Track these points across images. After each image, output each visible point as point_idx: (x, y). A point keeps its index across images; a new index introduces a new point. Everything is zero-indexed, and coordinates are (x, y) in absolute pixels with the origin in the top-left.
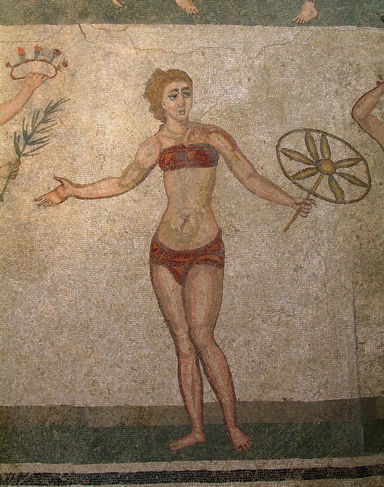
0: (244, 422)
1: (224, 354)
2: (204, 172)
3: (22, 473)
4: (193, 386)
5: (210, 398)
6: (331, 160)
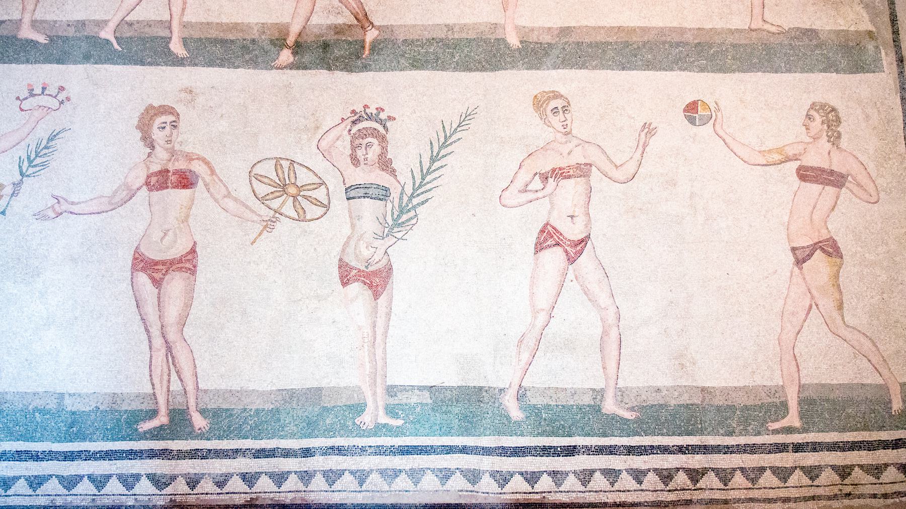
1: (191, 348)
2: (186, 192)
3: (5, 451)
4: (162, 375)
6: (297, 184)
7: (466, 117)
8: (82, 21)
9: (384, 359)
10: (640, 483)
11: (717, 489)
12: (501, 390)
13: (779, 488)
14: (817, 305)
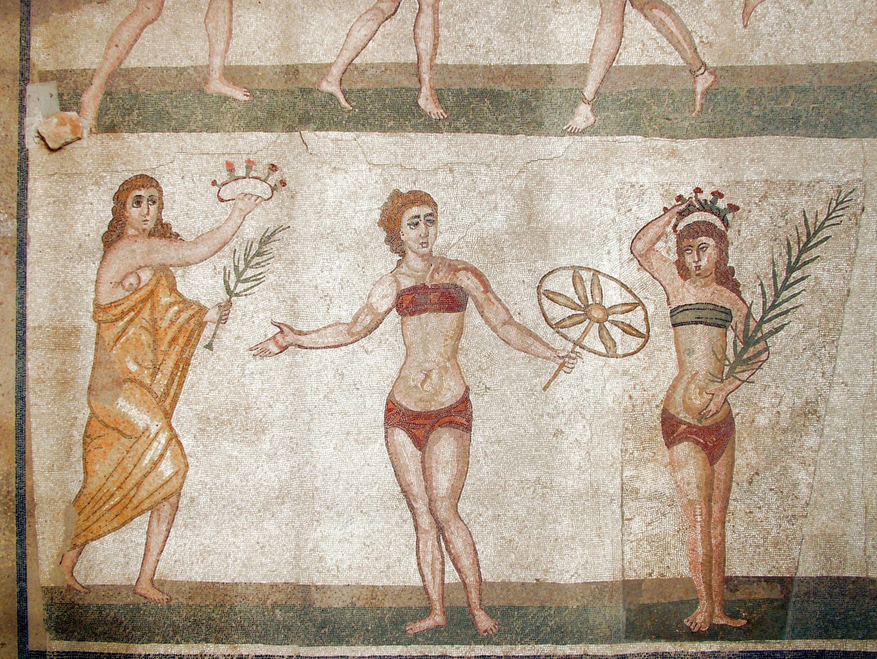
0: (490, 605)
2: (450, 318)
5: (451, 577)
7: (837, 205)
8: (293, 66)
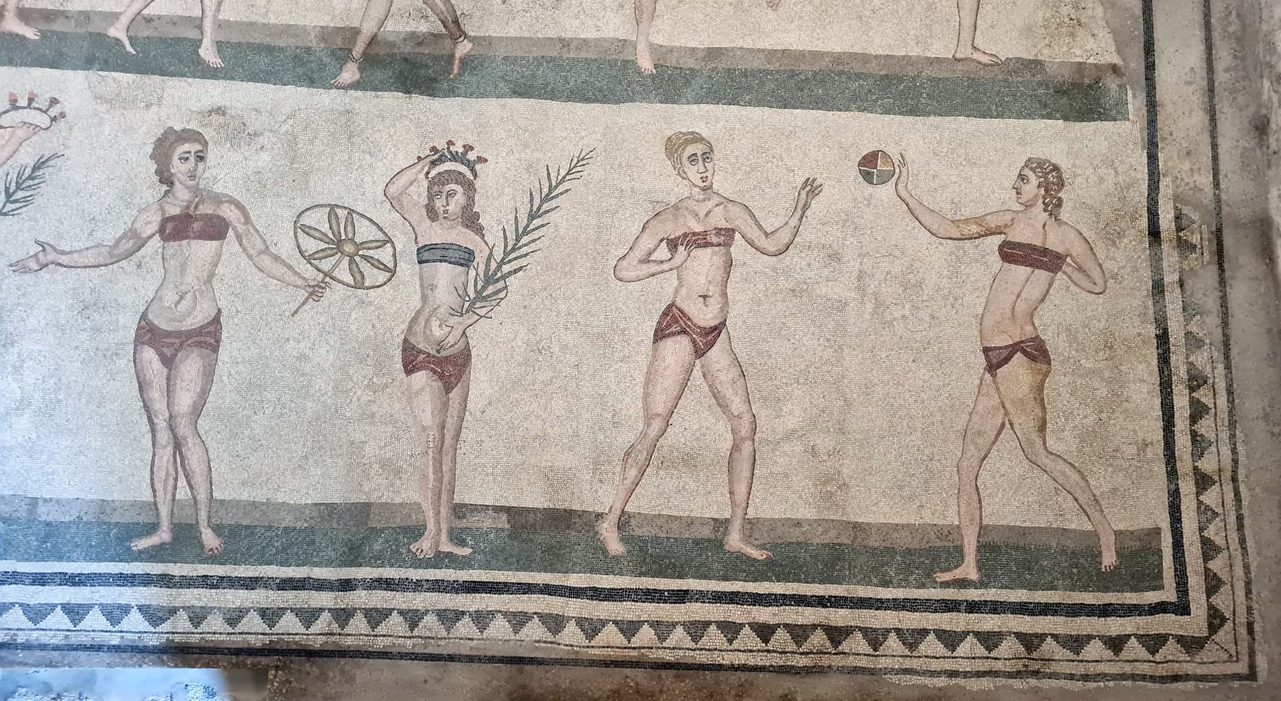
2: (212, 245)
4: (166, 480)
9: (453, 470)
10: (766, 641)
11: (865, 655)
12: (599, 516)
13: (944, 658)
14: (1011, 424)
